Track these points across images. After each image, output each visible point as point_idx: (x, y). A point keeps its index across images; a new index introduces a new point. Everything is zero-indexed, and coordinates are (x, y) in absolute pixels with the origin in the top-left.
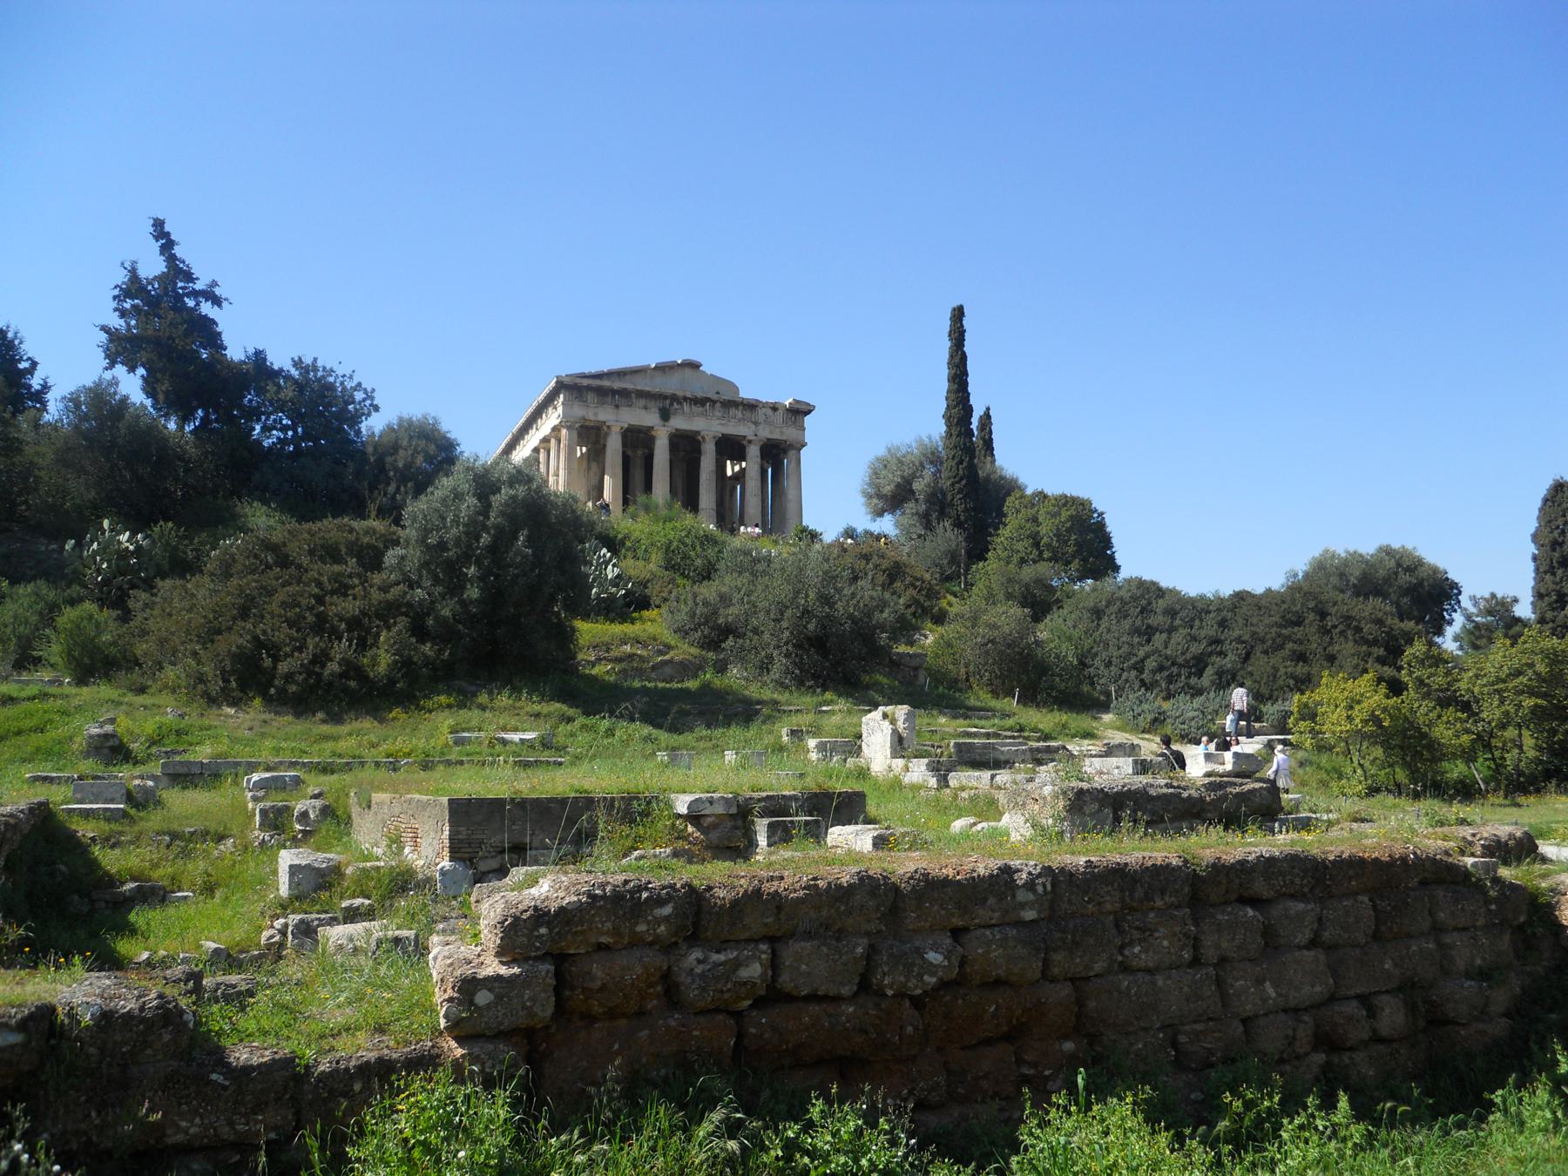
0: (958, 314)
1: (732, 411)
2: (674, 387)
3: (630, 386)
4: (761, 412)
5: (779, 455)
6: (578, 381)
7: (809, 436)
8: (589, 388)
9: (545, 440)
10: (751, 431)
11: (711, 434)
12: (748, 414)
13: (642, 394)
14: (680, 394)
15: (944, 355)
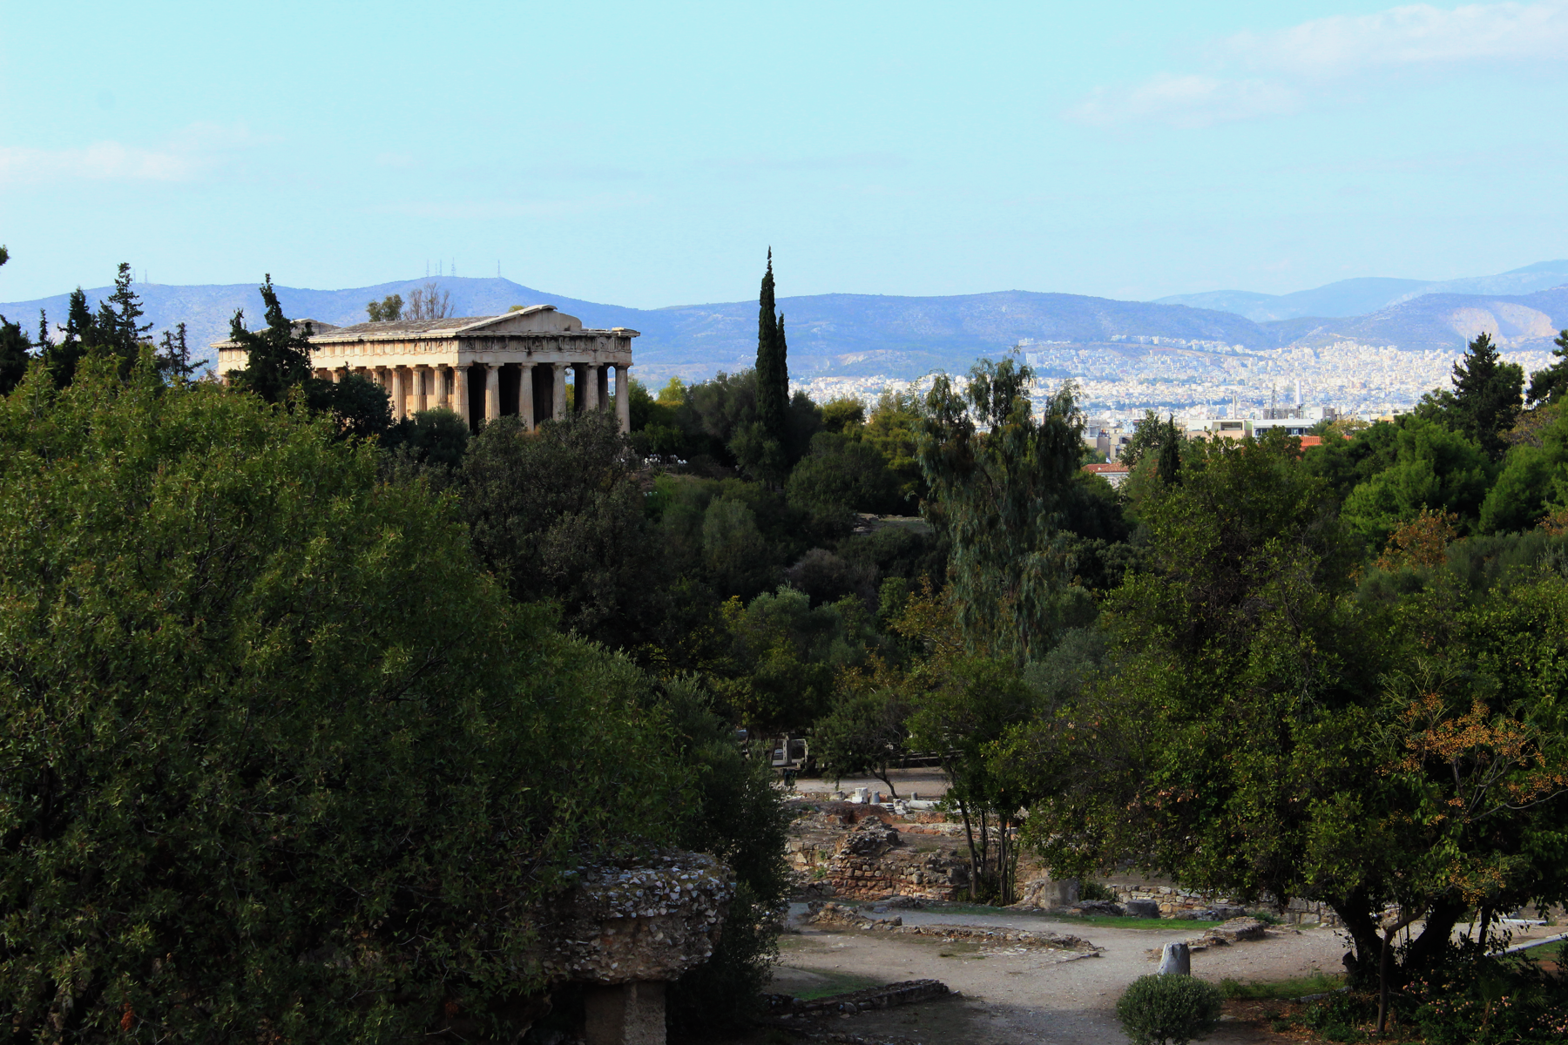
7: (634, 359)
9: (425, 371)
13: (513, 338)
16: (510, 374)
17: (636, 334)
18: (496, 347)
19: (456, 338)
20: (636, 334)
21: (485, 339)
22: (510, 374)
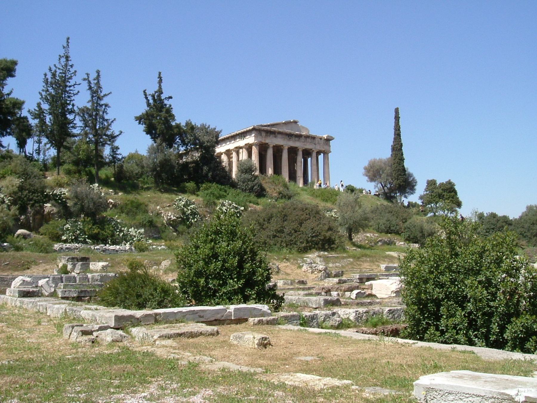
0: (397, 111)
1: (308, 139)
2: (289, 131)
3: (281, 130)
4: (317, 140)
8: (264, 130)
13: (280, 133)
15: (393, 124)
16: (278, 150)
17: (332, 139)
19: (254, 129)
20: (332, 139)
22: (278, 150)
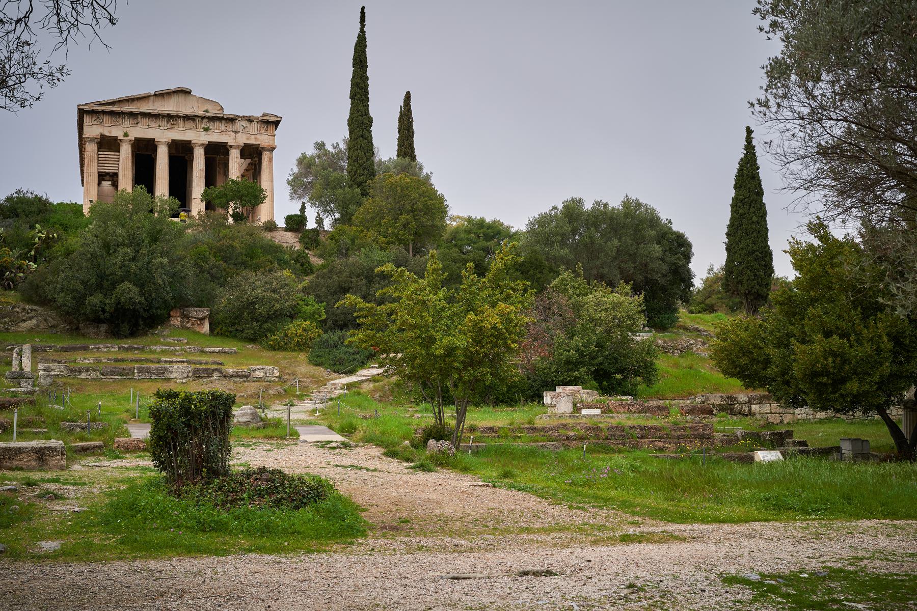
1: (217, 124)
5: (254, 155)
6: (96, 108)
7: (277, 142)
8: (103, 112)
10: (234, 138)
11: (201, 142)
12: (230, 127)
14: (174, 113)
18: (127, 122)
21: (112, 113)
